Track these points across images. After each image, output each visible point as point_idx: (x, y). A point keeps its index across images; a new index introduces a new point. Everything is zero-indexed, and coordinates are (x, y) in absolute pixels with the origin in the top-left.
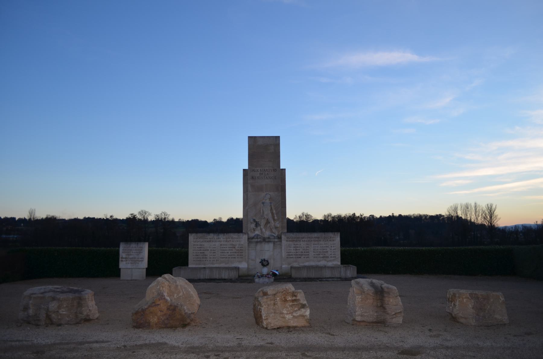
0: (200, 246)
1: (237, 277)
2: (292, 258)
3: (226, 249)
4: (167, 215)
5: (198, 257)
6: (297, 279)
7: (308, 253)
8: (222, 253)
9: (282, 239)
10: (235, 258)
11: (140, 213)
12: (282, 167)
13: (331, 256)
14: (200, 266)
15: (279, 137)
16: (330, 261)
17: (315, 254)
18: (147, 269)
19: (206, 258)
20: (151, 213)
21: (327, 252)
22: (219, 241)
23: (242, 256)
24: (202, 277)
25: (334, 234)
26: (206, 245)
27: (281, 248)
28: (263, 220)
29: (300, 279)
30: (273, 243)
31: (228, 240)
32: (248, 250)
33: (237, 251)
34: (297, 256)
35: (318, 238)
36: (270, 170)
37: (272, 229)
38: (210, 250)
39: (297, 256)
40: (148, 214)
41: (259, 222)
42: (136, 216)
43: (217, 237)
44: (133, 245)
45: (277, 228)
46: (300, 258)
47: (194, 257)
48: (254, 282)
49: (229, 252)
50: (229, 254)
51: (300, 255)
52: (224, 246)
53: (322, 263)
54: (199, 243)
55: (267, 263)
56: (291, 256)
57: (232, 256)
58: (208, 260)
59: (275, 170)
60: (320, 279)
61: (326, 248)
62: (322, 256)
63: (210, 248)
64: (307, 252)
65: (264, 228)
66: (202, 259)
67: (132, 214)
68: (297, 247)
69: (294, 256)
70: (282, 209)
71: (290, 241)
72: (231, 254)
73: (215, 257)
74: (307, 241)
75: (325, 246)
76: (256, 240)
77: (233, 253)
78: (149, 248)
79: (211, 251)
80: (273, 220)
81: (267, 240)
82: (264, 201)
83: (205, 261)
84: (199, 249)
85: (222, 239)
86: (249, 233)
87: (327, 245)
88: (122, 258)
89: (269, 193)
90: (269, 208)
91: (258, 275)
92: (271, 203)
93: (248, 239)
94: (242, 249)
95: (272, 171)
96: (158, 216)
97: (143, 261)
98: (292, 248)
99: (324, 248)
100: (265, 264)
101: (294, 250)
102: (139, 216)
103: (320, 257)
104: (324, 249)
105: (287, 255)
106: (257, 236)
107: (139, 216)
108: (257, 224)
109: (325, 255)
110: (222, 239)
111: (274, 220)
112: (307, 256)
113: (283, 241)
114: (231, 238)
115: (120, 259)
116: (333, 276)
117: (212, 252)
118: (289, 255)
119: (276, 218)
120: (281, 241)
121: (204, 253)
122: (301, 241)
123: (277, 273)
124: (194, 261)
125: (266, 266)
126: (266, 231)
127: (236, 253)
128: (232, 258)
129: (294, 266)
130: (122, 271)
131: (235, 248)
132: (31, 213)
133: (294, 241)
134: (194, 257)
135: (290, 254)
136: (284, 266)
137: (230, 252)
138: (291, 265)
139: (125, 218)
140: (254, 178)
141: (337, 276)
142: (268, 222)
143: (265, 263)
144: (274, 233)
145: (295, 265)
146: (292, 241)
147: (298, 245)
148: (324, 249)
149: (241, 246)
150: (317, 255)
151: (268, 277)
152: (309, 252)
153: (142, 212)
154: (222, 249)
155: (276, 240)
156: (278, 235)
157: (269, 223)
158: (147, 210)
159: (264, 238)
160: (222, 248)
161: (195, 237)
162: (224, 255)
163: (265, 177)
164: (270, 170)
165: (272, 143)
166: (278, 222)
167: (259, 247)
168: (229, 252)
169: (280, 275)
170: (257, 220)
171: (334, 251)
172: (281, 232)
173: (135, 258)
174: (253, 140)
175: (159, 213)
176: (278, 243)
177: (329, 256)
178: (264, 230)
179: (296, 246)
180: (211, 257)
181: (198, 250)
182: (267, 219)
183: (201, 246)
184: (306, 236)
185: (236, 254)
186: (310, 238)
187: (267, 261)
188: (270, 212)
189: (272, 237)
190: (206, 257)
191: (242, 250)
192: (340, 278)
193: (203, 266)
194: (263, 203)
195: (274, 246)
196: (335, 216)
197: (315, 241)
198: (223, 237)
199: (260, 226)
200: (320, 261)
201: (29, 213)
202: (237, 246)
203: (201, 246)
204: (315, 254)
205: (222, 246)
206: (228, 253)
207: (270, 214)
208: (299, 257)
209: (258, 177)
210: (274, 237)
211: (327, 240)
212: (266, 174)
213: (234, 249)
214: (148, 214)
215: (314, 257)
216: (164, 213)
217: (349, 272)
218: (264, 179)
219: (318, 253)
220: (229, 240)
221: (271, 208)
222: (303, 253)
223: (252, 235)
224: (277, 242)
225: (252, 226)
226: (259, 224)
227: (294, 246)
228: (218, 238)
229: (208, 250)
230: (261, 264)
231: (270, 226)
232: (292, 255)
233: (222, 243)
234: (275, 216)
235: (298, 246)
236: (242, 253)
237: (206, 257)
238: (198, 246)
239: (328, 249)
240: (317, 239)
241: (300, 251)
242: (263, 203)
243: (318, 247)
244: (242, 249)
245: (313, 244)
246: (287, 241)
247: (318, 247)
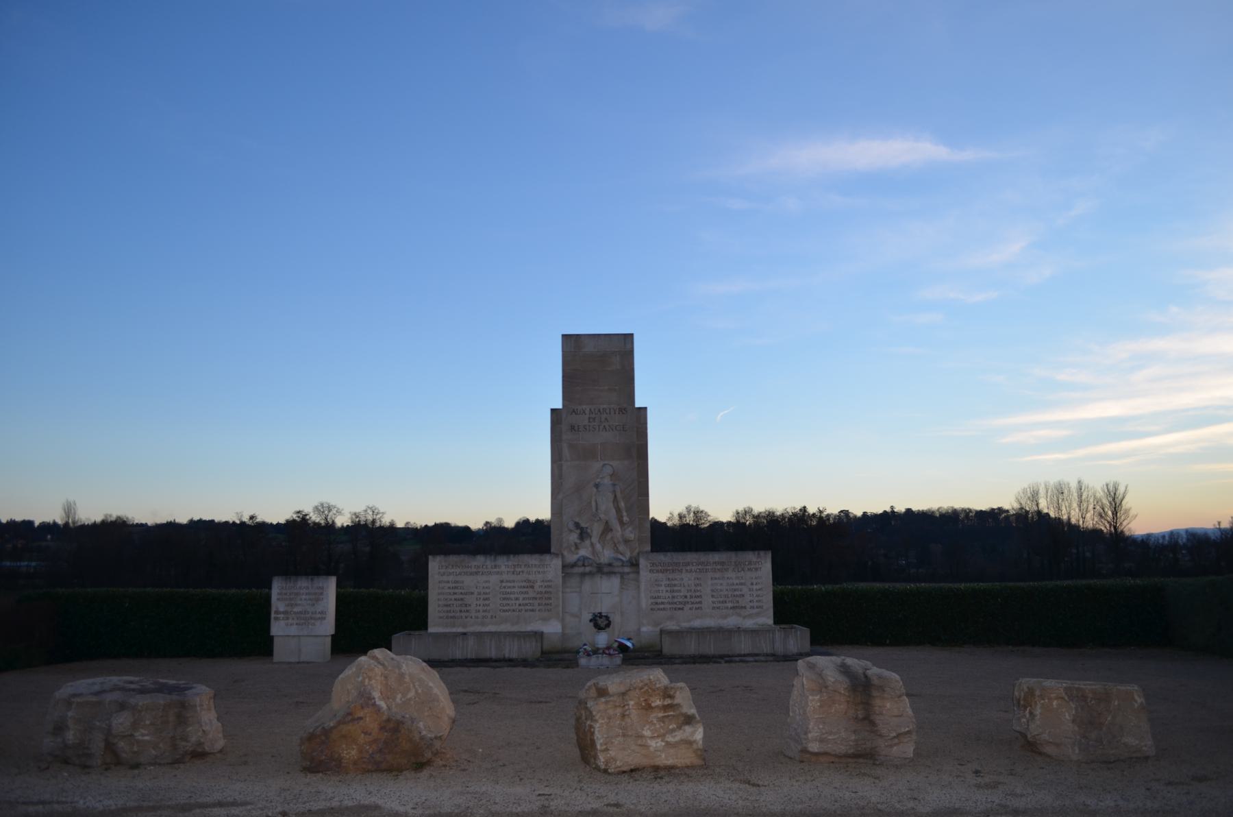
0: (454, 585)
1: (539, 654)
2: (664, 609)
4: (378, 513)
5: (449, 609)
6: (675, 658)
7: (698, 600)
8: (504, 599)
9: (641, 566)
11: (316, 509)
12: (639, 403)
13: (751, 604)
14: (454, 630)
15: (632, 335)
16: (750, 616)
17: (715, 600)
18: (334, 638)
19: (467, 611)
20: (343, 510)
21: (743, 596)
22: (498, 573)
23: (549, 607)
24: (458, 655)
25: (759, 554)
26: (468, 581)
27: (639, 587)
28: (596, 524)
29: (681, 657)
30: (619, 576)
31: (518, 570)
32: (563, 592)
33: (539, 596)
34: (675, 606)
35: (722, 563)
36: (612, 412)
37: (618, 545)
38: (476, 593)
39: (675, 606)
40: (335, 512)
41: (587, 528)
42: (308, 517)
44: (303, 583)
45: (629, 541)
46: (681, 611)
48: (577, 665)
49: (521, 599)
50: (521, 601)
51: (681, 603)
52: (509, 584)
53: (732, 621)
54: (451, 578)
55: (607, 622)
56: (662, 606)
57: (527, 607)
58: (471, 617)
59: (622, 411)
60: (727, 659)
61: (740, 587)
62: (730, 605)
63: (477, 588)
64: (698, 597)
65: (599, 543)
66: (458, 614)
67: (299, 512)
68: (675, 585)
69: (668, 606)
70: (640, 498)
71: (658, 571)
72: (524, 602)
73: (488, 608)
74: (696, 572)
75: (738, 581)
76: (581, 570)
77: (529, 599)
78: (339, 590)
79: (479, 596)
80: (620, 524)
81: (606, 570)
82: (598, 480)
83: (466, 617)
84: (452, 591)
85: (503, 567)
86: (565, 553)
87: (743, 581)
88: (277, 612)
89: (611, 464)
90: (611, 496)
91: (585, 649)
92: (614, 485)
93: (564, 566)
94: (550, 590)
95: (617, 413)
96: (357, 517)
97: (325, 618)
98: (663, 588)
99: (734, 587)
100: (603, 625)
101: (667, 591)
102: (316, 515)
103: (727, 608)
104: (735, 590)
105: (652, 603)
106: (583, 561)
107: (316, 515)
108: (583, 534)
109: (738, 602)
110: (503, 568)
111: (622, 523)
112: (697, 606)
113: (641, 572)
114: (525, 565)
115: (273, 615)
116: (756, 651)
117: (482, 597)
118: (657, 603)
119: (625, 519)
120: (638, 573)
121: (462, 599)
122: (684, 571)
123: (629, 644)
124: (441, 618)
125: (604, 629)
126: (603, 549)
127: (536, 599)
128: (526, 611)
129: (668, 628)
130: (276, 642)
131: (532, 587)
132: (69, 509)
133: (667, 570)
135: (659, 601)
136: (644, 629)
137: (521, 597)
138: (662, 626)
139: (282, 521)
140: (576, 428)
141: (765, 651)
142: (607, 529)
143: (602, 622)
144: (621, 554)
145: (671, 626)
146: (662, 571)
147: (676, 579)
148: (735, 590)
149: (546, 584)
150: (720, 602)
151: (610, 654)
152: (700, 597)
153: (323, 508)
154: (503, 590)
155: (627, 570)
156: (631, 558)
157: (611, 530)
158: (332, 503)
159: (600, 564)
160: (505, 587)
162: (509, 605)
163: (601, 427)
164: (612, 412)
165: (616, 350)
166: (630, 529)
167: (587, 585)
168: (521, 599)
169: (635, 650)
170: (583, 525)
171: (759, 592)
172: (637, 551)
173: (306, 612)
174: (572, 344)
175: (359, 509)
176: (632, 576)
177: (748, 606)
178: (598, 547)
179: (673, 582)
180: (478, 608)
181: (450, 594)
182: (607, 522)
183: (456, 585)
184: (695, 561)
185: (536, 602)
186: (702, 563)
187: (607, 618)
188: (611, 505)
189: (620, 564)
191: (550, 593)
192: (773, 655)
193: (461, 630)
194: (597, 486)
195: (622, 583)
196: (760, 513)
197: (714, 571)
198: (506, 563)
199: (591, 537)
200: (725, 617)
201: (65, 512)
202: (539, 584)
203: (456, 585)
204: (715, 600)
205: (504, 584)
206: (517, 599)
207: (614, 511)
208: (679, 609)
209: (584, 426)
210: (620, 564)
211: (743, 570)
212: (603, 419)
214: (337, 512)
215: (714, 608)
216: (371, 508)
217: (792, 642)
218: (599, 431)
219: (721, 600)
220: (520, 570)
221: (615, 496)
222: (688, 600)
223: (571, 558)
224: (628, 573)
225: (571, 538)
226: (587, 533)
227: (668, 582)
228: (495, 566)
229: (472, 593)
230: (592, 624)
231: (612, 538)
232: (663, 603)
233: (505, 577)
234: (625, 514)
235: (676, 582)
236: (550, 598)
239: (745, 590)
240: (719, 567)
241: (682, 594)
242: (597, 486)
243: (721, 584)
244: (550, 590)
245: (712, 579)
246: (651, 571)
247: (721, 584)
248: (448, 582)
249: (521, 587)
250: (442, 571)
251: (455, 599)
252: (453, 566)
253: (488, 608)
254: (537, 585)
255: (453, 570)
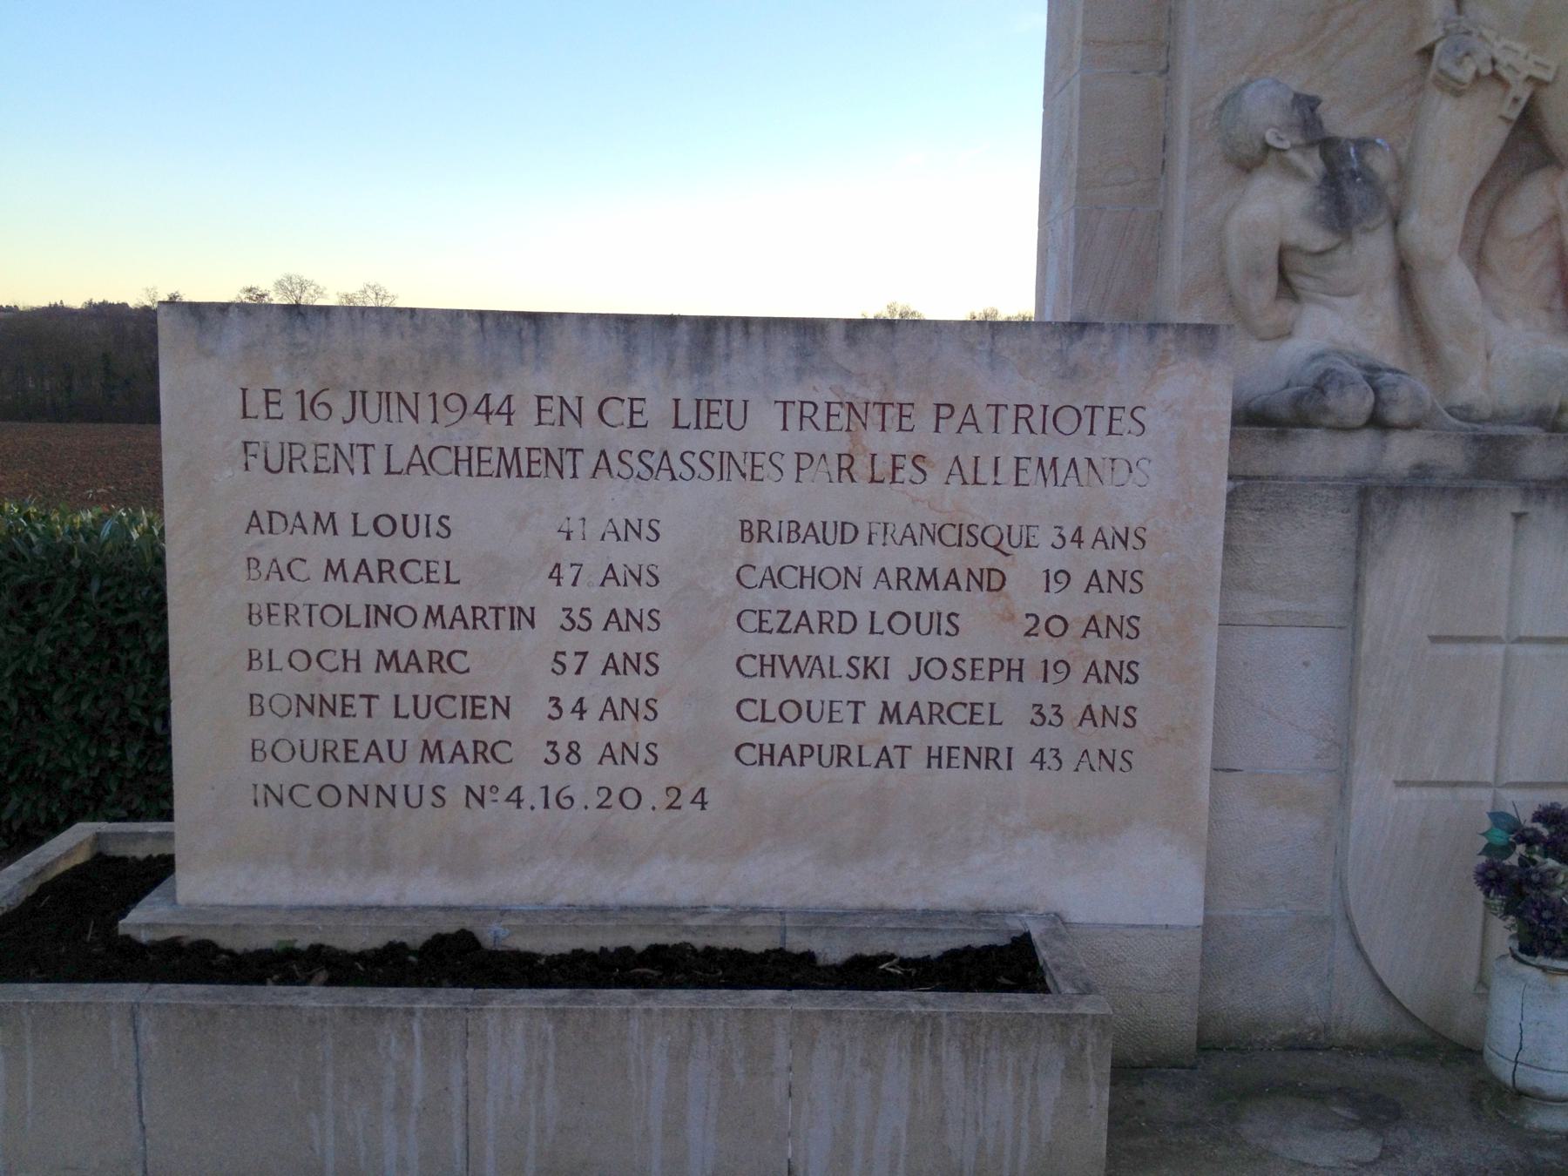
0: (372, 548)
3: (839, 600)
5: (337, 728)
8: (769, 665)
10: (985, 758)
19: (484, 751)
23: (1114, 738)
31: (884, 442)
33: (1044, 647)
38: (548, 617)
41: (1362, 144)
43: (684, 390)
47: (268, 728)
50: (897, 689)
52: (810, 555)
57: (944, 734)
58: (516, 797)
63: (556, 575)
66: (412, 772)
72: (925, 692)
73: (646, 732)
77: (964, 669)
79: (573, 642)
83: (475, 797)
84: (356, 595)
94: (1119, 604)
121: (441, 661)
124: (273, 796)
127: (1014, 670)
128: (935, 758)
131: (990, 581)
134: (268, 728)
137: (903, 650)
149: (1102, 559)
154: (766, 597)
160: (775, 578)
161: (279, 378)
162: (804, 710)
168: (902, 666)
170: (1339, 121)
180: (569, 728)
181: (345, 616)
183: (397, 548)
185: (1014, 698)
190: (493, 729)
191: (1129, 627)
196: (1411, 268)
198: (797, 394)
202: (1044, 557)
203: (397, 548)
205: (768, 554)
206: (868, 668)
213: (971, 605)
220: (896, 442)
226: (1365, 176)
228: (705, 414)
229: (522, 617)
236: (1126, 672)
237: (493, 729)
238: (322, 547)
248: (326, 523)
249: (902, 578)
250: (270, 433)
251: (388, 661)
252: (358, 399)
253: (646, 732)
254: (1025, 569)
255: (360, 431)
